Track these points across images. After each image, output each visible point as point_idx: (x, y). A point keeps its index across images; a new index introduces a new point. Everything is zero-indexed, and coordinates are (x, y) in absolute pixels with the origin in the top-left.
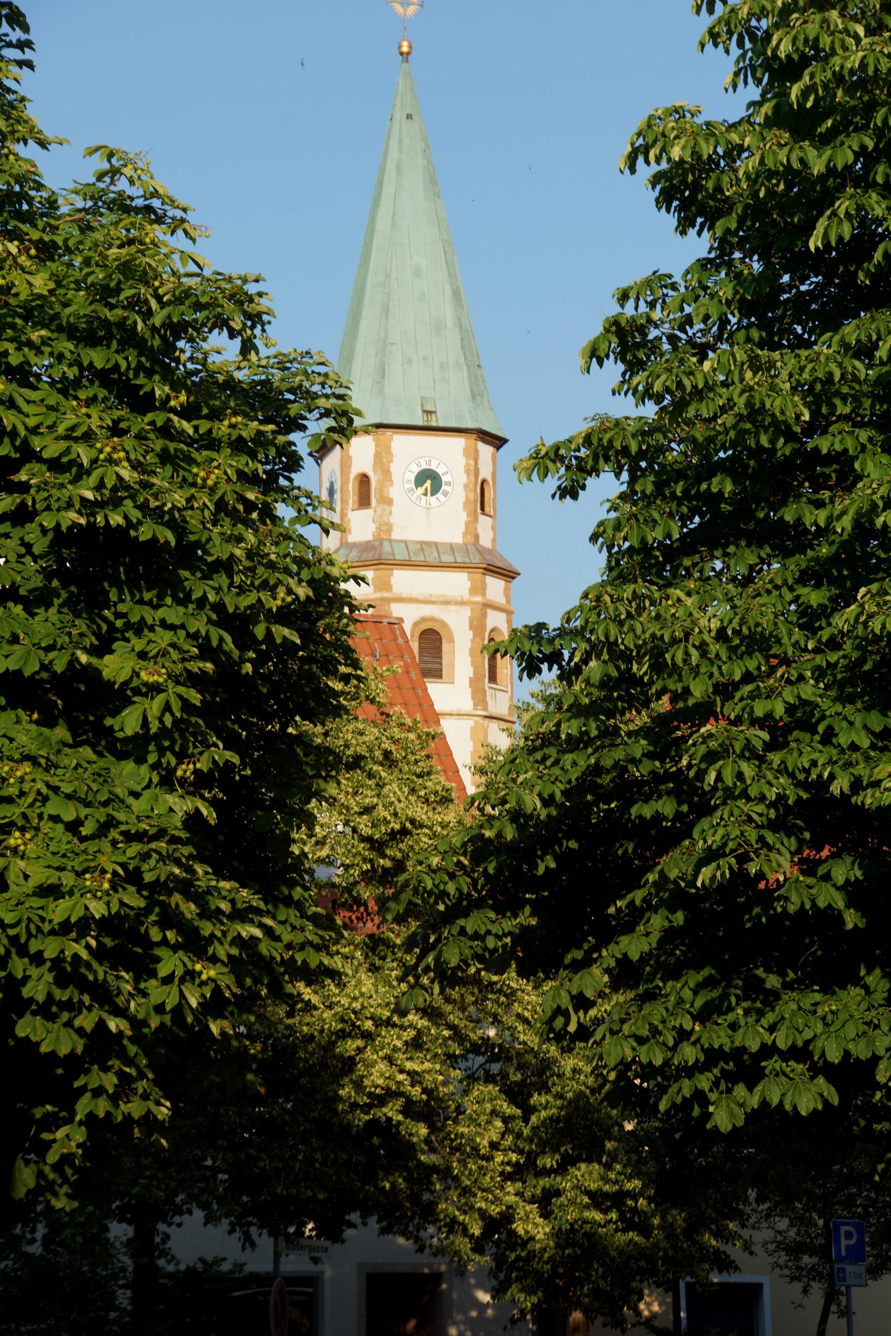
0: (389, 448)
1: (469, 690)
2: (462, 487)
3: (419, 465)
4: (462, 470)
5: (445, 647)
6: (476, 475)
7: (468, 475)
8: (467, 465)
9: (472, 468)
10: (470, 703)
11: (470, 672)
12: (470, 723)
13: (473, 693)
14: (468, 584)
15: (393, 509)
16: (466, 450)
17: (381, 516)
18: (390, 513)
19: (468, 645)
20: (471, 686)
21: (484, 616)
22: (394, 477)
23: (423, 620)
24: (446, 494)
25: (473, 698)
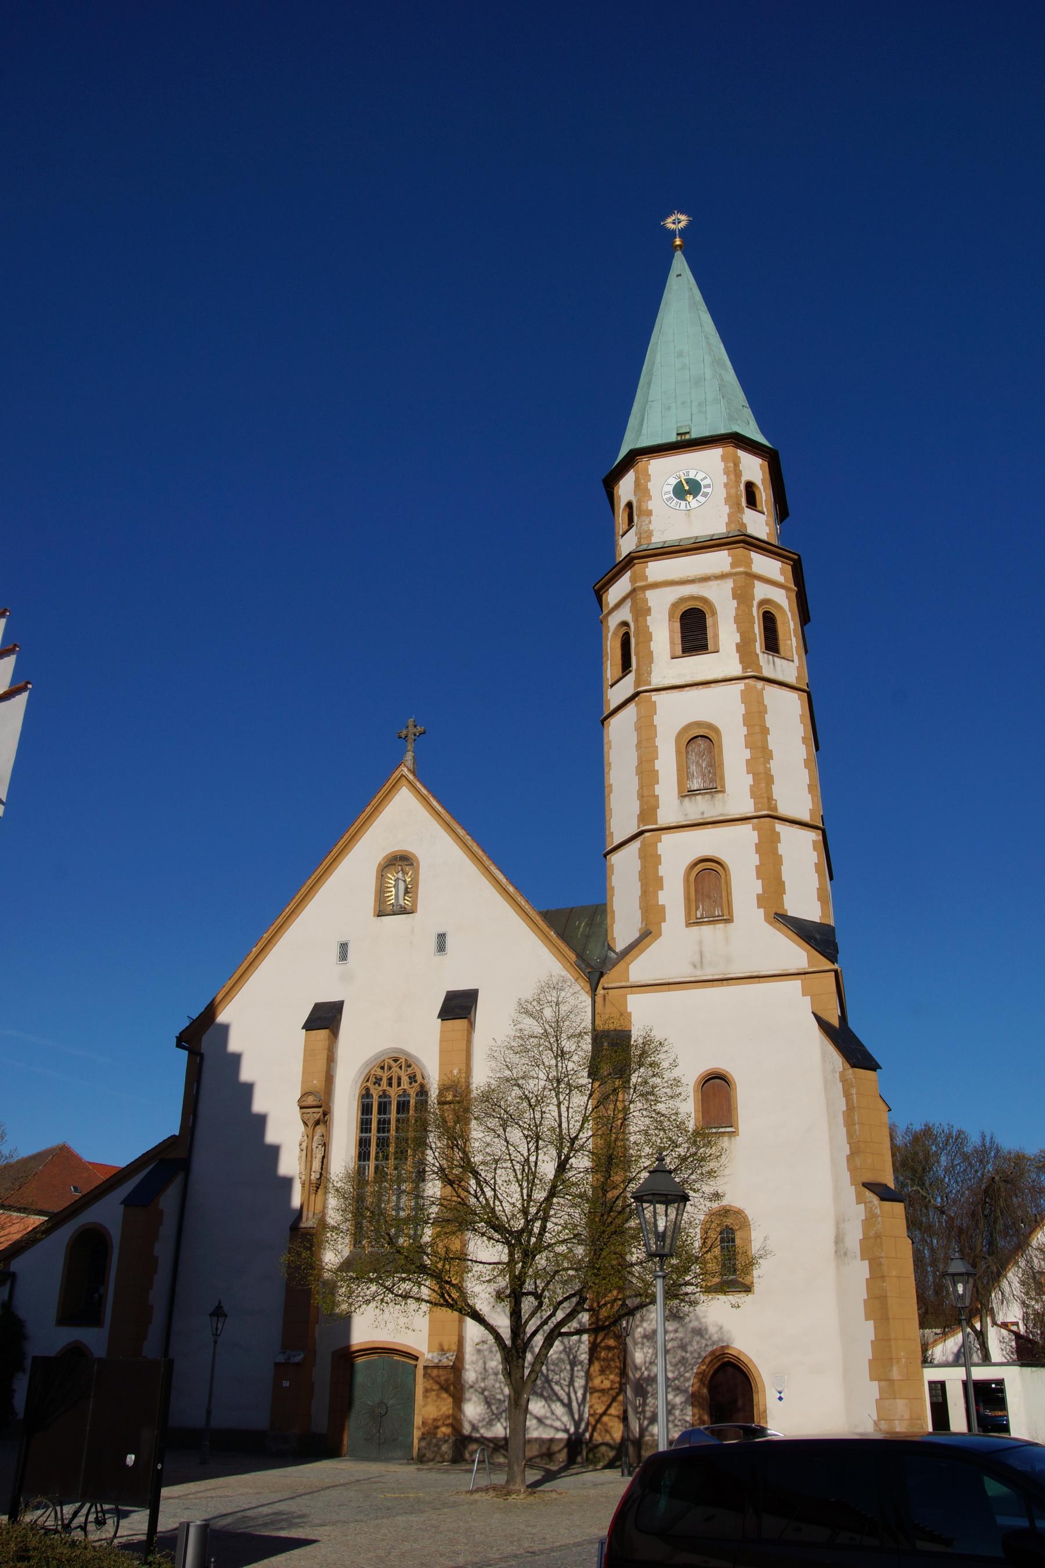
5: (709, 621)
6: (738, 474)
8: (726, 467)
9: (731, 469)
11: (737, 639)
14: (730, 560)
15: (652, 518)
16: (724, 458)
18: (650, 522)
20: (738, 651)
23: (682, 600)
24: (705, 495)
25: (741, 662)
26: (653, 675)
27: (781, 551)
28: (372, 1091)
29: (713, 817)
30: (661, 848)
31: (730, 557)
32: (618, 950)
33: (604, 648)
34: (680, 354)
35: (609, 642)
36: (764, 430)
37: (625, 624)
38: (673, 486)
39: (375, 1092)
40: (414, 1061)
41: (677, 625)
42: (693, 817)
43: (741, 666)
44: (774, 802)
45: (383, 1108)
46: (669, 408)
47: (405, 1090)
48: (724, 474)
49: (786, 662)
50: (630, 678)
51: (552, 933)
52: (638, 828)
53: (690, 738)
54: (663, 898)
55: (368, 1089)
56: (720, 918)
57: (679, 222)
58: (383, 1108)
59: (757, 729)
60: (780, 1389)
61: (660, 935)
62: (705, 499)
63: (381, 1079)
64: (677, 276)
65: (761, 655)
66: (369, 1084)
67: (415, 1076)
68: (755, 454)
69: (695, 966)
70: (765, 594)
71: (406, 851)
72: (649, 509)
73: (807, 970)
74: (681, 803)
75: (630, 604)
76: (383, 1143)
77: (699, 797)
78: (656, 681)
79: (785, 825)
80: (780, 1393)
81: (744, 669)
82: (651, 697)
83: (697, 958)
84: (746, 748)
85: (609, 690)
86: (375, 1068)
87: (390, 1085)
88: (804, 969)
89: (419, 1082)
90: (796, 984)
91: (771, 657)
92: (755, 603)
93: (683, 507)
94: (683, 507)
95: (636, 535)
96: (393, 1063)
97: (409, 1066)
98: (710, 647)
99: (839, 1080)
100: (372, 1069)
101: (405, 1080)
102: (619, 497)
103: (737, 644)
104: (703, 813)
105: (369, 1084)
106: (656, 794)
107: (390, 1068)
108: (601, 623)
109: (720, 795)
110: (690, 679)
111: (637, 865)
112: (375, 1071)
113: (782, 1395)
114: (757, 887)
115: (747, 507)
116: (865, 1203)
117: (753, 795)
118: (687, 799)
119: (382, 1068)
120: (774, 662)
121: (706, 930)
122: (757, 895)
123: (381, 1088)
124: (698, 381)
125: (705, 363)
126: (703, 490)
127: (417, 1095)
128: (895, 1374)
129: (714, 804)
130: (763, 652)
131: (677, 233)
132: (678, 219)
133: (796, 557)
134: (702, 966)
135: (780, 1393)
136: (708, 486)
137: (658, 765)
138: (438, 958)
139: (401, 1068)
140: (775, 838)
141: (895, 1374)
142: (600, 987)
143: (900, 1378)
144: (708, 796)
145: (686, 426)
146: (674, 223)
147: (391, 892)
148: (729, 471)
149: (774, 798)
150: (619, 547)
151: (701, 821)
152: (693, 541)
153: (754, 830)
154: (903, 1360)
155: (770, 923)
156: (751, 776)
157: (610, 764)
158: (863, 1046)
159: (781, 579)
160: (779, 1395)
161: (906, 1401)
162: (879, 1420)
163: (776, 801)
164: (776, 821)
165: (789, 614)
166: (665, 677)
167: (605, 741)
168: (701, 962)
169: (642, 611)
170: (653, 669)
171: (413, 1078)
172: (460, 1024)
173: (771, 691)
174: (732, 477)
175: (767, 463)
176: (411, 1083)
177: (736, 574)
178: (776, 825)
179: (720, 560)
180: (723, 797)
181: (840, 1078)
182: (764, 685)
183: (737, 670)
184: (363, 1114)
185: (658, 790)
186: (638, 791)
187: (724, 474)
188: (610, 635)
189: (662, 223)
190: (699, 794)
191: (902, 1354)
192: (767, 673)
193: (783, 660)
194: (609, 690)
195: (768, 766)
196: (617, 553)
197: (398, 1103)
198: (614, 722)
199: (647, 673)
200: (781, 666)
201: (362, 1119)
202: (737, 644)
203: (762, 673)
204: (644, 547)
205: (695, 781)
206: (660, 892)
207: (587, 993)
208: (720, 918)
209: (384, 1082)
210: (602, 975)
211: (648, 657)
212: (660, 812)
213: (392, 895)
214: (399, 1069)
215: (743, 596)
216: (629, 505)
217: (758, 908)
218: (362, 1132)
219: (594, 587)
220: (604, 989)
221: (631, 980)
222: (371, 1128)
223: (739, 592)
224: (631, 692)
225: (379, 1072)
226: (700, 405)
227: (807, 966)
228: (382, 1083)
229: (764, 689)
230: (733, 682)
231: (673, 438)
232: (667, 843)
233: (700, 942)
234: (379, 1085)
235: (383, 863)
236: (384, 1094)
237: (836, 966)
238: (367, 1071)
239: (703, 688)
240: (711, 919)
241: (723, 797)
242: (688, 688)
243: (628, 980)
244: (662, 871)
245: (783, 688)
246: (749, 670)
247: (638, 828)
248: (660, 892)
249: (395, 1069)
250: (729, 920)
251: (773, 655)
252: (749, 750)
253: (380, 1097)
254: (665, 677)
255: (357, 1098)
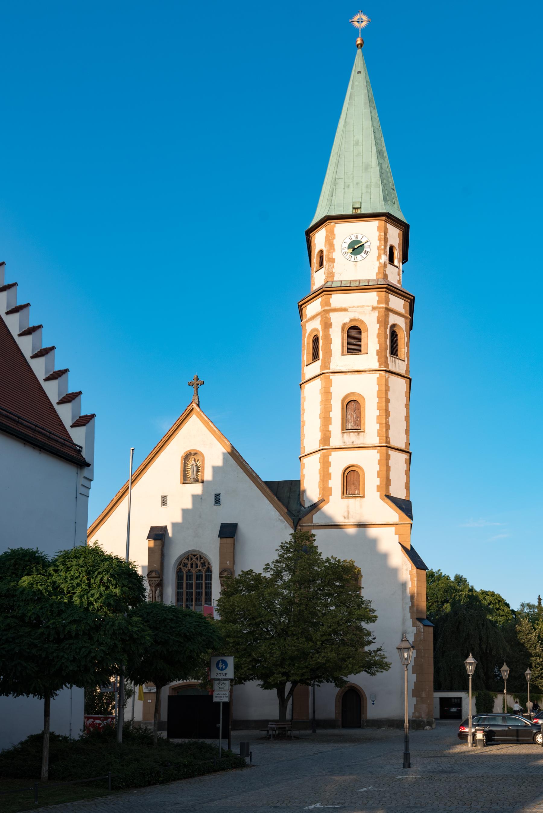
0: (333, 231)
1: (377, 357)
2: (376, 248)
3: (351, 238)
4: (377, 238)
5: (363, 335)
6: (386, 240)
7: (380, 241)
8: (380, 235)
9: (383, 237)
10: (377, 364)
12: (376, 375)
13: (379, 359)
14: (377, 298)
15: (335, 264)
16: (379, 229)
17: (328, 269)
18: (333, 267)
19: (377, 332)
20: (377, 355)
21: (387, 316)
22: (336, 247)
24: (366, 253)
25: (379, 361)
26: (331, 364)
27: (405, 294)
28: (183, 570)
29: (358, 444)
30: (331, 459)
31: (378, 297)
32: (306, 506)
33: (303, 342)
34: (357, 143)
35: (306, 339)
36: (403, 208)
37: (316, 330)
38: (348, 244)
39: (184, 571)
40: (204, 556)
41: (346, 335)
42: (348, 444)
43: (378, 363)
44: (389, 439)
45: (189, 577)
46: (349, 186)
47: (200, 570)
48: (378, 240)
49: (401, 361)
50: (318, 364)
51: (275, 498)
52: (319, 447)
53: (348, 401)
54: (331, 483)
55: (180, 569)
56: (358, 495)
57: (362, 22)
58: (189, 577)
59: (384, 400)
60: (373, 700)
61: (329, 502)
62: (366, 256)
63: (187, 564)
64: (358, 73)
65: (389, 357)
66: (181, 566)
67: (205, 563)
68: (397, 227)
69: (345, 518)
70: (394, 321)
71: (197, 450)
72: (334, 258)
73: (398, 523)
74: (343, 436)
75: (320, 319)
76: (189, 594)
77: (352, 434)
78: (333, 367)
79: (393, 451)
80: (373, 701)
81: (380, 365)
82: (329, 376)
83: (346, 514)
84: (377, 409)
85: (305, 368)
86: (184, 559)
87: (192, 567)
88: (397, 522)
89: (207, 566)
90: (393, 529)
91: (394, 359)
92: (389, 327)
93: (353, 259)
94: (353, 259)
95: (325, 274)
96: (193, 557)
97: (202, 558)
98: (363, 351)
99: (409, 574)
100: (182, 560)
101: (199, 564)
102: (315, 245)
103: (377, 350)
104: (353, 442)
105: (181, 566)
106: (330, 430)
107: (192, 559)
108: (302, 328)
109: (362, 434)
110: (351, 368)
111: (318, 466)
112: (184, 560)
113: (374, 702)
114: (377, 481)
115: (389, 263)
116: (416, 627)
117: (379, 435)
118: (345, 434)
119: (188, 559)
120: (395, 361)
121: (351, 500)
122: (377, 485)
123: (187, 569)
124: (367, 167)
125: (372, 152)
126: (365, 249)
127: (206, 572)
128: (424, 695)
129: (359, 438)
130: (390, 356)
131: (360, 32)
132: (362, 19)
133: (412, 298)
134: (348, 518)
135: (373, 701)
136: (368, 247)
137: (332, 414)
138: (216, 507)
139: (197, 559)
140: (388, 457)
141: (424, 695)
142: (298, 525)
143: (426, 696)
144: (356, 434)
145: (358, 202)
146: (358, 22)
147: (189, 471)
148: (381, 238)
149: (389, 437)
150: (313, 279)
151: (352, 446)
152: (357, 284)
153: (378, 453)
154: (427, 690)
155: (383, 499)
156: (378, 425)
157: (304, 410)
158: (421, 559)
159: (403, 311)
160: (372, 702)
161: (427, 705)
162: (415, 712)
163: (390, 438)
164: (389, 449)
165: (405, 333)
166: (338, 366)
167: (302, 396)
168: (348, 516)
169: (327, 325)
170: (331, 360)
171: (203, 564)
172: (229, 541)
173: (393, 378)
174: (383, 242)
175: (402, 232)
176: (203, 567)
177: (380, 308)
178: (389, 451)
179: (372, 297)
180: (364, 435)
181: (410, 573)
182: (389, 375)
183: (376, 366)
184: (178, 580)
185: (331, 428)
186: (320, 427)
187: (378, 240)
188: (307, 335)
189: (350, 21)
190: (352, 432)
191: (427, 687)
192: (391, 368)
193: (399, 360)
194: (305, 368)
195: (388, 420)
196: (312, 283)
197: (197, 576)
198: (307, 386)
199: (328, 362)
200: (399, 364)
201: (178, 583)
202: (377, 350)
203: (388, 368)
204: (329, 284)
205: (350, 424)
206: (329, 481)
207: (292, 528)
208: (358, 495)
209: (189, 565)
210: (300, 519)
211: (328, 353)
212: (331, 440)
213: (190, 475)
214: (196, 560)
215: (383, 321)
216: (321, 252)
217: (377, 492)
218: (178, 589)
219: (298, 304)
220: (300, 526)
221: (314, 522)
222: (183, 587)
223: (381, 319)
224: (318, 372)
225: (186, 561)
226: (367, 187)
227: (398, 521)
228: (188, 566)
229: (389, 377)
230: (373, 372)
231: (350, 212)
232: (334, 457)
233: (348, 507)
234: (187, 567)
235: (184, 455)
236: (189, 571)
237: (411, 522)
238: (180, 561)
239: (357, 374)
240: (354, 495)
241: (364, 435)
242: (349, 373)
243: (312, 523)
244: (331, 470)
245: (399, 376)
246: (382, 366)
247: (319, 447)
248: (329, 481)
249: (194, 559)
250: (363, 497)
251: (395, 358)
252: (379, 410)
253: (187, 573)
254: (338, 366)
255: (175, 573)
